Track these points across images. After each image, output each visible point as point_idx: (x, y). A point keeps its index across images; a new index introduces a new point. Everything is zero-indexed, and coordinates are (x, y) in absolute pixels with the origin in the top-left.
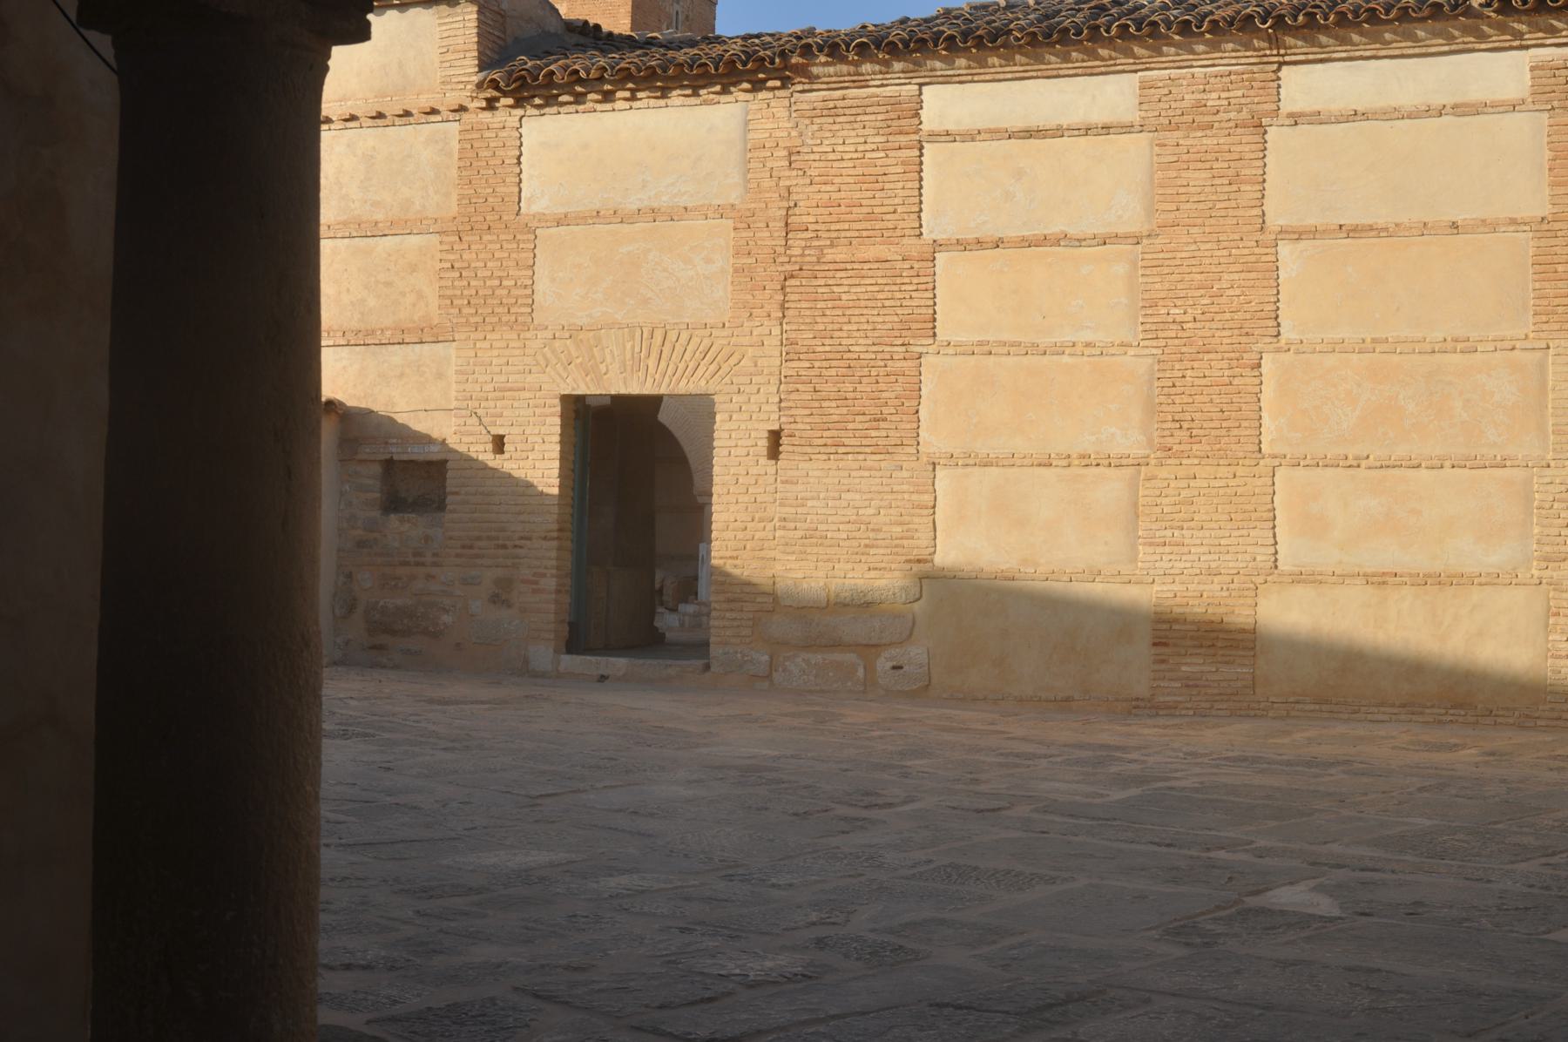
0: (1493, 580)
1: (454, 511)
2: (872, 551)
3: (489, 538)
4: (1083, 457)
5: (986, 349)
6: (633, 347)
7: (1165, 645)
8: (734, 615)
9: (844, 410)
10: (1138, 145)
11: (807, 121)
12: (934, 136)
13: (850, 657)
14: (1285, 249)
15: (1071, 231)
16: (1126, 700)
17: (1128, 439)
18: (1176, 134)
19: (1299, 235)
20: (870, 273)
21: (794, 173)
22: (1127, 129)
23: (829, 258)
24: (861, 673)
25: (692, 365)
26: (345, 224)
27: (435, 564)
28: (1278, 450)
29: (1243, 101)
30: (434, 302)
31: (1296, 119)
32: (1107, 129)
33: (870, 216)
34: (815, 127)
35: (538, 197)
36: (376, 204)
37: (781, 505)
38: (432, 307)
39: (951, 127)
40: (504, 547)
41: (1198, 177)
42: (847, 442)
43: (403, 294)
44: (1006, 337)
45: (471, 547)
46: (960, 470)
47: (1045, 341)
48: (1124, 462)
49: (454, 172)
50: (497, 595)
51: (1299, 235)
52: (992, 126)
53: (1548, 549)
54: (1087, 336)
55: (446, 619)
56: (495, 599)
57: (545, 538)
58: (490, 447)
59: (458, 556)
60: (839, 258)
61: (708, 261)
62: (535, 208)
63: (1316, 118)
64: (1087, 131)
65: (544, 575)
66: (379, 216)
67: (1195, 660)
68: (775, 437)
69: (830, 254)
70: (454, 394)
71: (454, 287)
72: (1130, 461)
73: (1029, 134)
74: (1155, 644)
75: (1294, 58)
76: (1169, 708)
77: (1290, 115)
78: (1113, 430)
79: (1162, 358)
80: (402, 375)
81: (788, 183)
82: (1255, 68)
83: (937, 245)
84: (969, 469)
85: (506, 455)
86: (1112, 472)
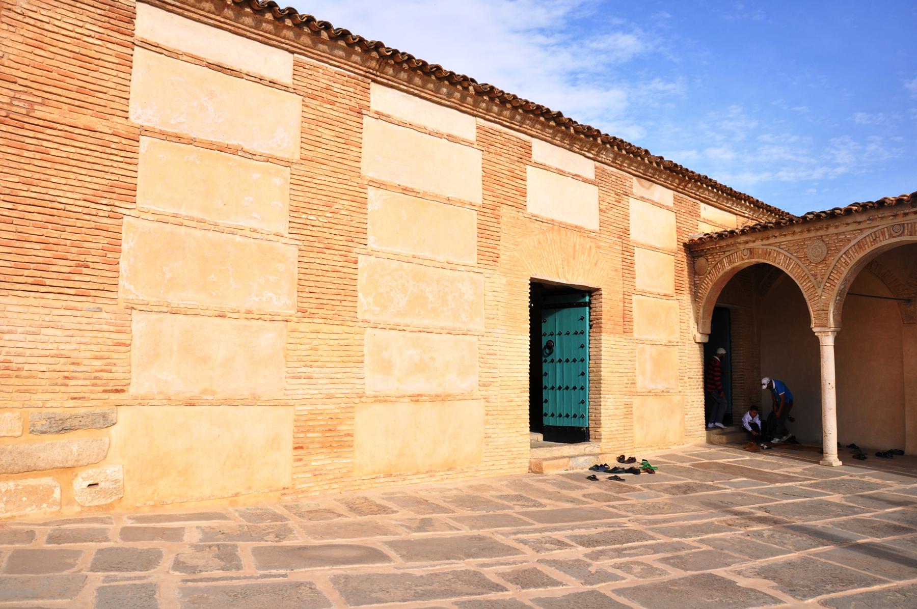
0: (463, 397)
2: (72, 382)
4: (250, 312)
5: (177, 221)
7: (301, 448)
9: (48, 254)
10: (294, 103)
12: (147, 45)
13: (46, 481)
14: (371, 192)
15: (246, 148)
16: (277, 490)
17: (283, 300)
18: (315, 102)
19: (380, 185)
22: (286, 88)
24: (57, 494)
28: (367, 317)
33: (81, 90)
41: (328, 134)
42: (48, 282)
44: (195, 214)
46: (154, 316)
48: (277, 318)
51: (380, 185)
53: (484, 380)
54: (254, 224)
60: (48, 117)
67: (319, 457)
72: (280, 318)
74: (296, 448)
75: (382, 80)
76: (303, 492)
77: (377, 113)
78: (270, 294)
79: (303, 248)
82: (360, 78)
83: (145, 131)
84: (162, 315)
86: (268, 324)
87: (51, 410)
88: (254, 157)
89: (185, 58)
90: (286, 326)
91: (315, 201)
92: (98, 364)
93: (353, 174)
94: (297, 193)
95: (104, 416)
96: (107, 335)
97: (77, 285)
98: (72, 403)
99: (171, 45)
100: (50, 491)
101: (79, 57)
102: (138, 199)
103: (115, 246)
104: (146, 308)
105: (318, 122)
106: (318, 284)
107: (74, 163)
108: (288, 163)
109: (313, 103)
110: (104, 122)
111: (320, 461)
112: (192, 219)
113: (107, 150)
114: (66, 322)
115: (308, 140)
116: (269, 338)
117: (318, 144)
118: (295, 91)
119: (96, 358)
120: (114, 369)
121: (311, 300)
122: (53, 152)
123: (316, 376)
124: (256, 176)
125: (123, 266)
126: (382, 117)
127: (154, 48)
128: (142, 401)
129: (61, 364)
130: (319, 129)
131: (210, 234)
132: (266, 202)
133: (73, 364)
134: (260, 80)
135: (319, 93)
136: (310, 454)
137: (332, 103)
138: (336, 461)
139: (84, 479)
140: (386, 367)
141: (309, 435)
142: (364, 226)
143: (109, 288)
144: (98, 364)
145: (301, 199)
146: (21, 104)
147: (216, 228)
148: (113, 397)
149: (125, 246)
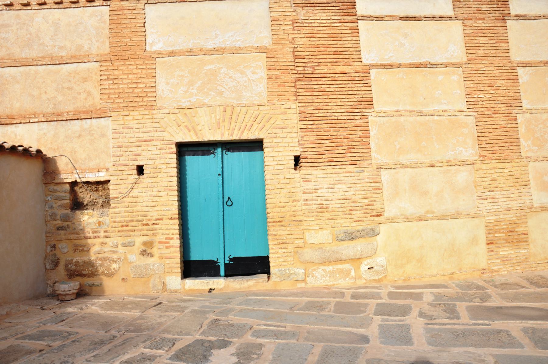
1: (116, 207)
2: (354, 213)
3: (137, 221)
4: (449, 161)
5: (398, 114)
6: (216, 116)
7: (492, 243)
8: (284, 250)
9: (333, 145)
11: (301, 9)
12: (365, 18)
13: (346, 266)
14: (520, 71)
15: (432, 61)
16: (478, 270)
17: (469, 151)
18: (471, 21)
19: (526, 65)
20: (340, 79)
21: (296, 32)
22: (450, 18)
23: (317, 72)
24: (353, 273)
25: (249, 125)
26: (43, 58)
27: (106, 237)
28: (529, 154)
29: (497, 9)
30: (97, 96)
31: (518, 17)
32: (441, 18)
34: (305, 12)
35: (155, 42)
36: (61, 48)
37: (304, 193)
38: (95, 100)
39: (372, 14)
40: (147, 225)
41: (483, 40)
42: (335, 160)
43: (79, 94)
44: (409, 108)
45: (127, 226)
46: (393, 171)
47: (425, 110)
48: (467, 163)
49: (107, 31)
50: (145, 251)
51: (526, 65)
52: (391, 14)
54: (445, 107)
55: (115, 266)
56: (144, 253)
57: (171, 219)
58: (135, 172)
59: (119, 231)
60: (322, 72)
61: (254, 73)
62: (155, 48)
64: (433, 18)
65: (172, 238)
66: (63, 54)
67: (505, 249)
68: (297, 159)
69: (318, 70)
70: (111, 145)
71: (110, 89)
72: (469, 163)
74: (488, 244)
76: (496, 271)
77: (516, 16)
78: (461, 149)
79: (478, 116)
80: (80, 136)
81: (293, 36)
83: (372, 66)
84: (398, 170)
85: (145, 176)
86: (462, 168)
87: (345, 228)
88: (438, 66)
89: (387, 18)
90: (474, 167)
91: (481, 85)
92: (366, 201)
93: (504, 62)
94: (468, 83)
95: (373, 230)
96: (368, 184)
97: (350, 159)
98: (355, 224)
99: (377, 14)
100: (349, 271)
101: (331, 35)
102: (375, 106)
103: (366, 135)
104: (388, 167)
106: (491, 138)
107: (338, 93)
108: (459, 65)
109: (469, 23)
110: (350, 67)
111: (505, 251)
112: (407, 111)
113: (354, 82)
114: (347, 180)
115: (470, 47)
116: (463, 176)
117: (478, 48)
118: (457, 18)
119: (365, 198)
120: (375, 203)
121: (488, 149)
122: (327, 90)
123: (497, 197)
124: (441, 78)
125: (372, 145)
126: (520, 18)
127: (368, 19)
128: (392, 220)
129: (347, 203)
130: (477, 38)
131: (418, 118)
132: (449, 93)
133: (353, 202)
134: (433, 18)
135: (473, 15)
136: (498, 247)
137: (483, 19)
138: (517, 251)
139: (366, 265)
141: (496, 235)
142: (518, 94)
143: (366, 158)
144: (366, 201)
145: (472, 85)
146: (309, 69)
147: (422, 114)
148: (376, 219)
149: (372, 134)
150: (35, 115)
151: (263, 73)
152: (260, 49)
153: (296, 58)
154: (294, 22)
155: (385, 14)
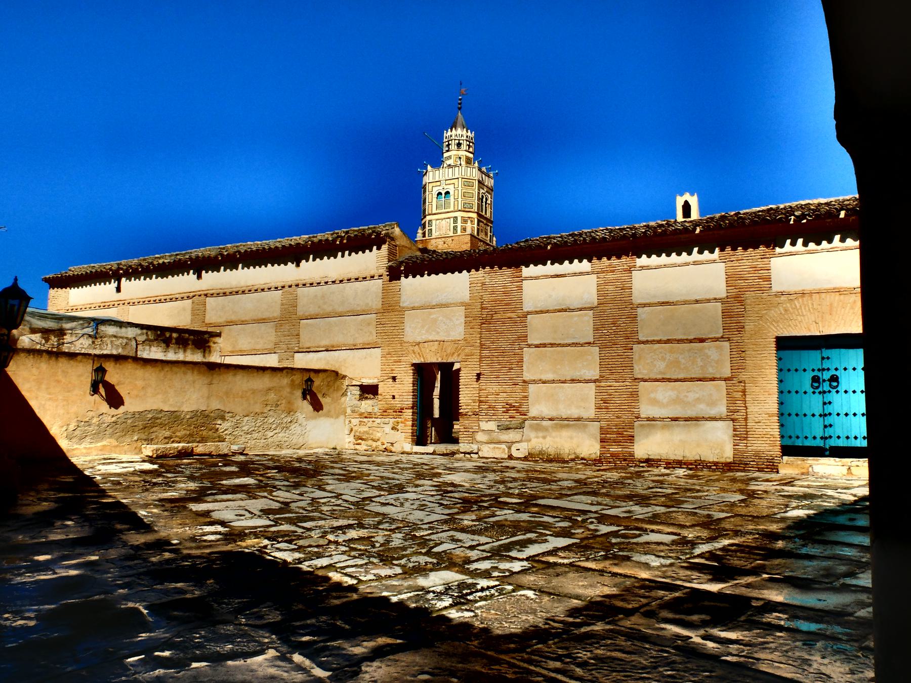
13: (503, 446)
22: (588, 273)
35: (405, 301)
62: (405, 305)
63: (648, 268)
68: (479, 376)
73: (557, 276)
83: (529, 313)
103: (521, 361)
104: (534, 382)
105: (606, 284)
108: (591, 309)
109: (601, 275)
118: (593, 273)
125: (524, 368)
128: (534, 418)
140: (655, 402)
150: (345, 345)
151: (463, 320)
152: (462, 304)
153: (482, 308)
154: (483, 284)
155: (540, 274)
